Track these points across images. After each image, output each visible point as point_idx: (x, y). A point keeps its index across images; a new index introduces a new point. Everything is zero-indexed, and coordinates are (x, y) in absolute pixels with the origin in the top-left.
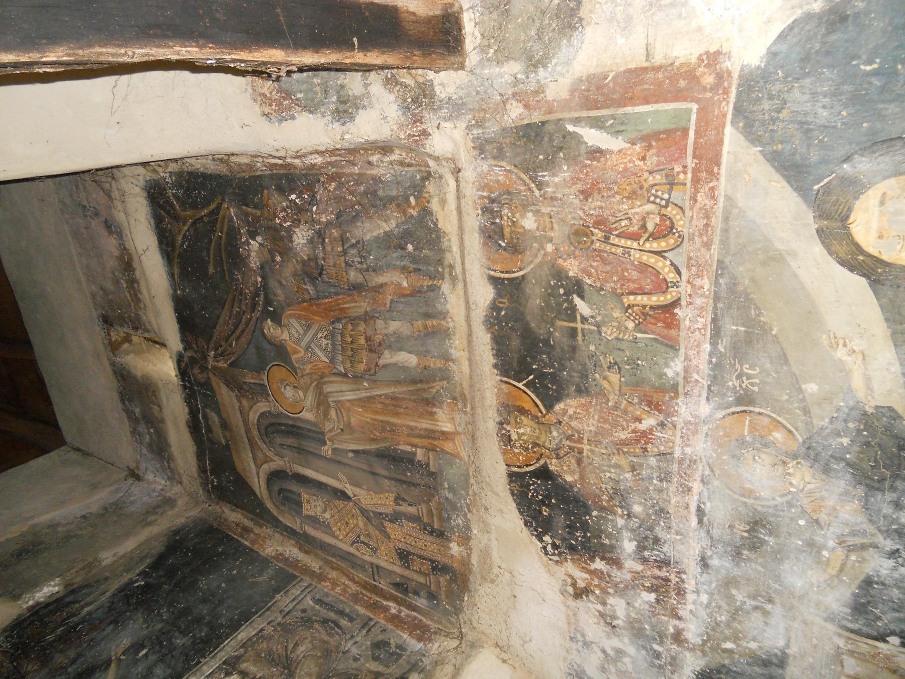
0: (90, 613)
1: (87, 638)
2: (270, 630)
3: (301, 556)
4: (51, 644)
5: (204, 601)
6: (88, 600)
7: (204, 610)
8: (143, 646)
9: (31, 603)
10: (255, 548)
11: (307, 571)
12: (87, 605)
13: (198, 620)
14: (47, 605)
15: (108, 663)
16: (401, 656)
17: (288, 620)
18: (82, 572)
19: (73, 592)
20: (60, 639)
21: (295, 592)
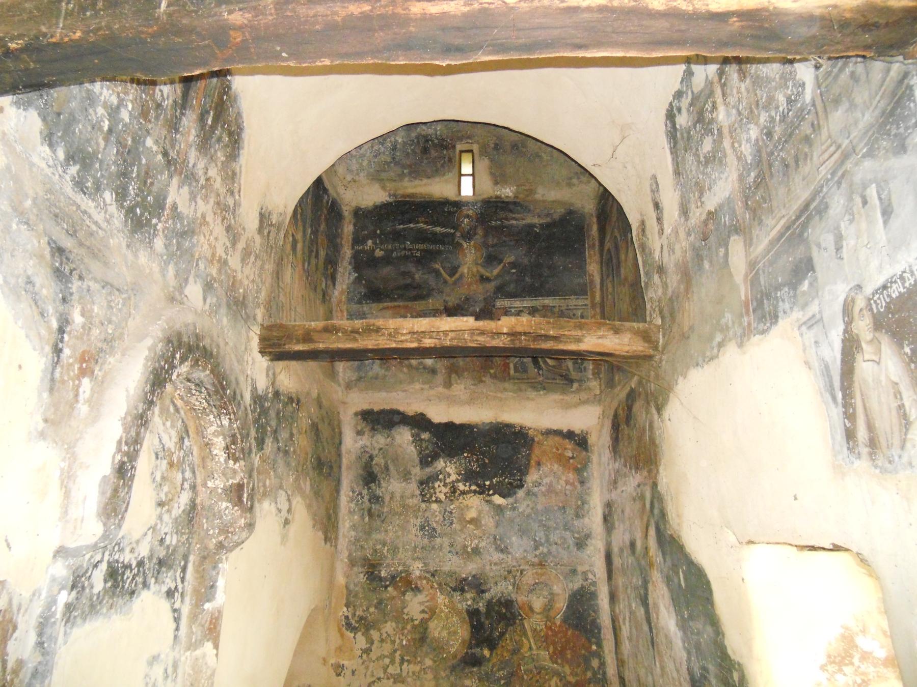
0: (512, 225)
1: (504, 238)
2: (556, 310)
3: (598, 287)
4: (492, 227)
5: (549, 268)
6: (516, 216)
7: (546, 272)
8: (514, 267)
9: (498, 193)
10: (588, 260)
11: (593, 297)
12: (514, 219)
13: (540, 276)
14: (503, 202)
15: (501, 261)
16: (581, 372)
17: (566, 312)
18: (526, 193)
19: (515, 203)
20: (496, 228)
21: (580, 302)
